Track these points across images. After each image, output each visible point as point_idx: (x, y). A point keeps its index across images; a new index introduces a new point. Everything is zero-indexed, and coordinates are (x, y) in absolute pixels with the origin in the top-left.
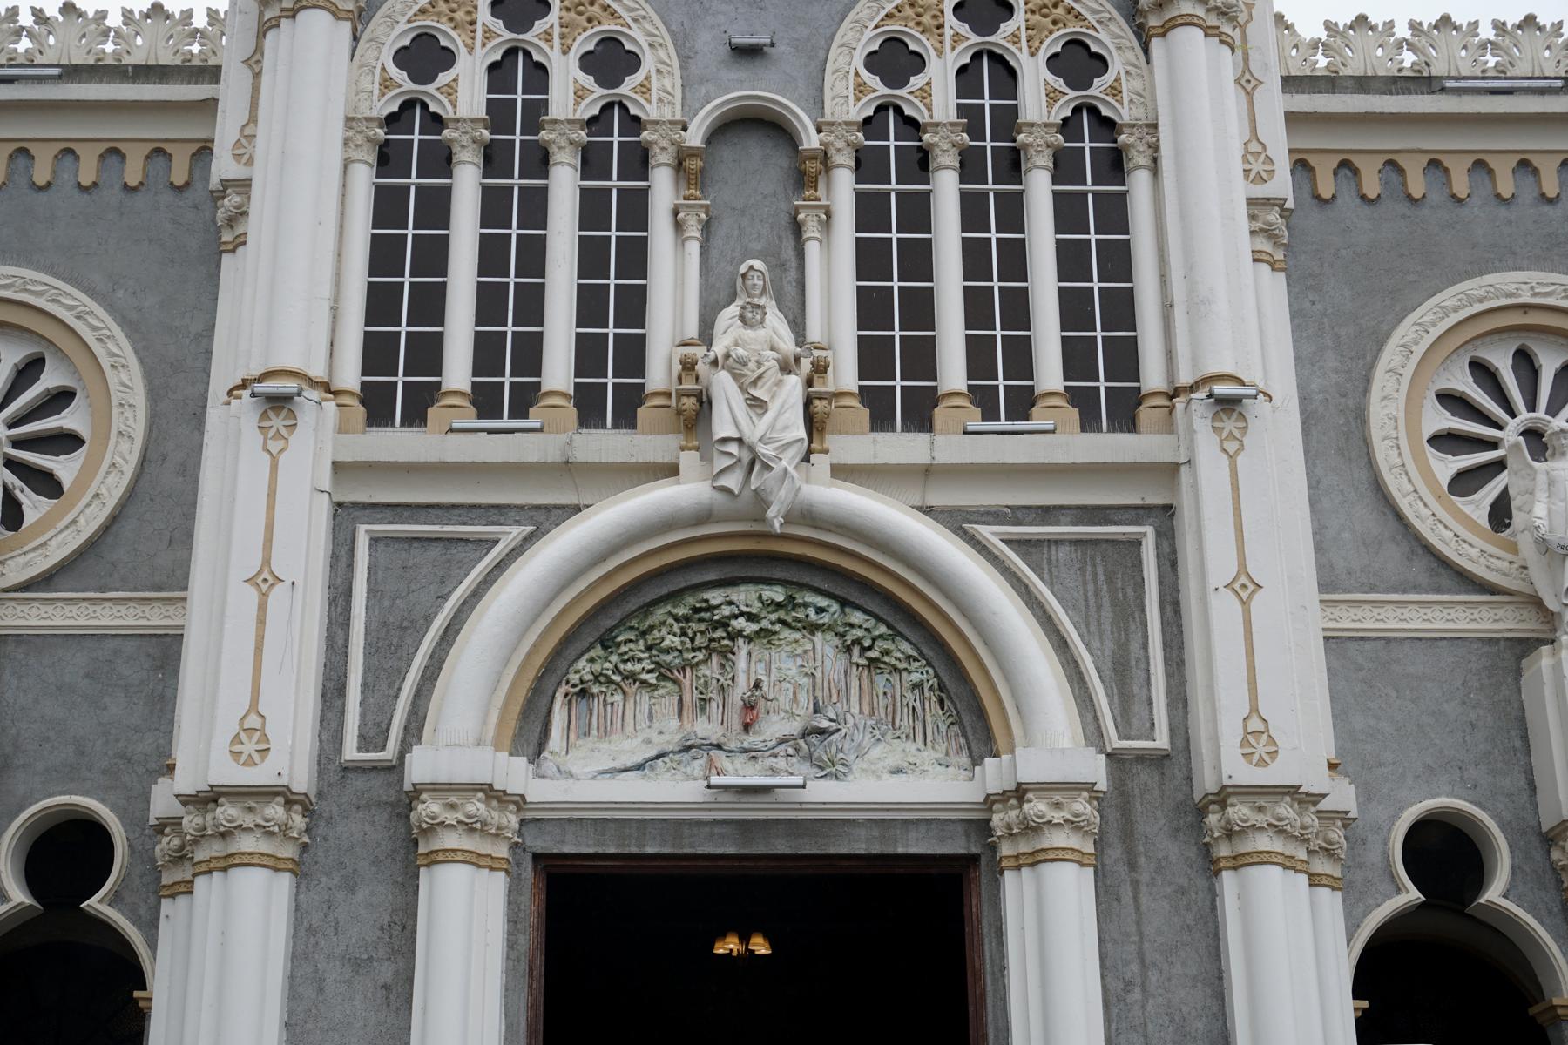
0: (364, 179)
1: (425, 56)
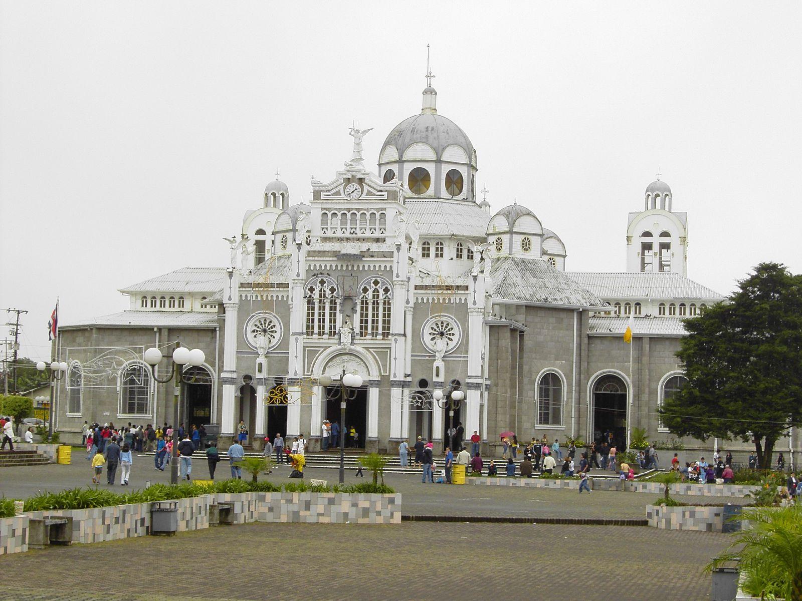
0: (306, 306)
1: (312, 290)
